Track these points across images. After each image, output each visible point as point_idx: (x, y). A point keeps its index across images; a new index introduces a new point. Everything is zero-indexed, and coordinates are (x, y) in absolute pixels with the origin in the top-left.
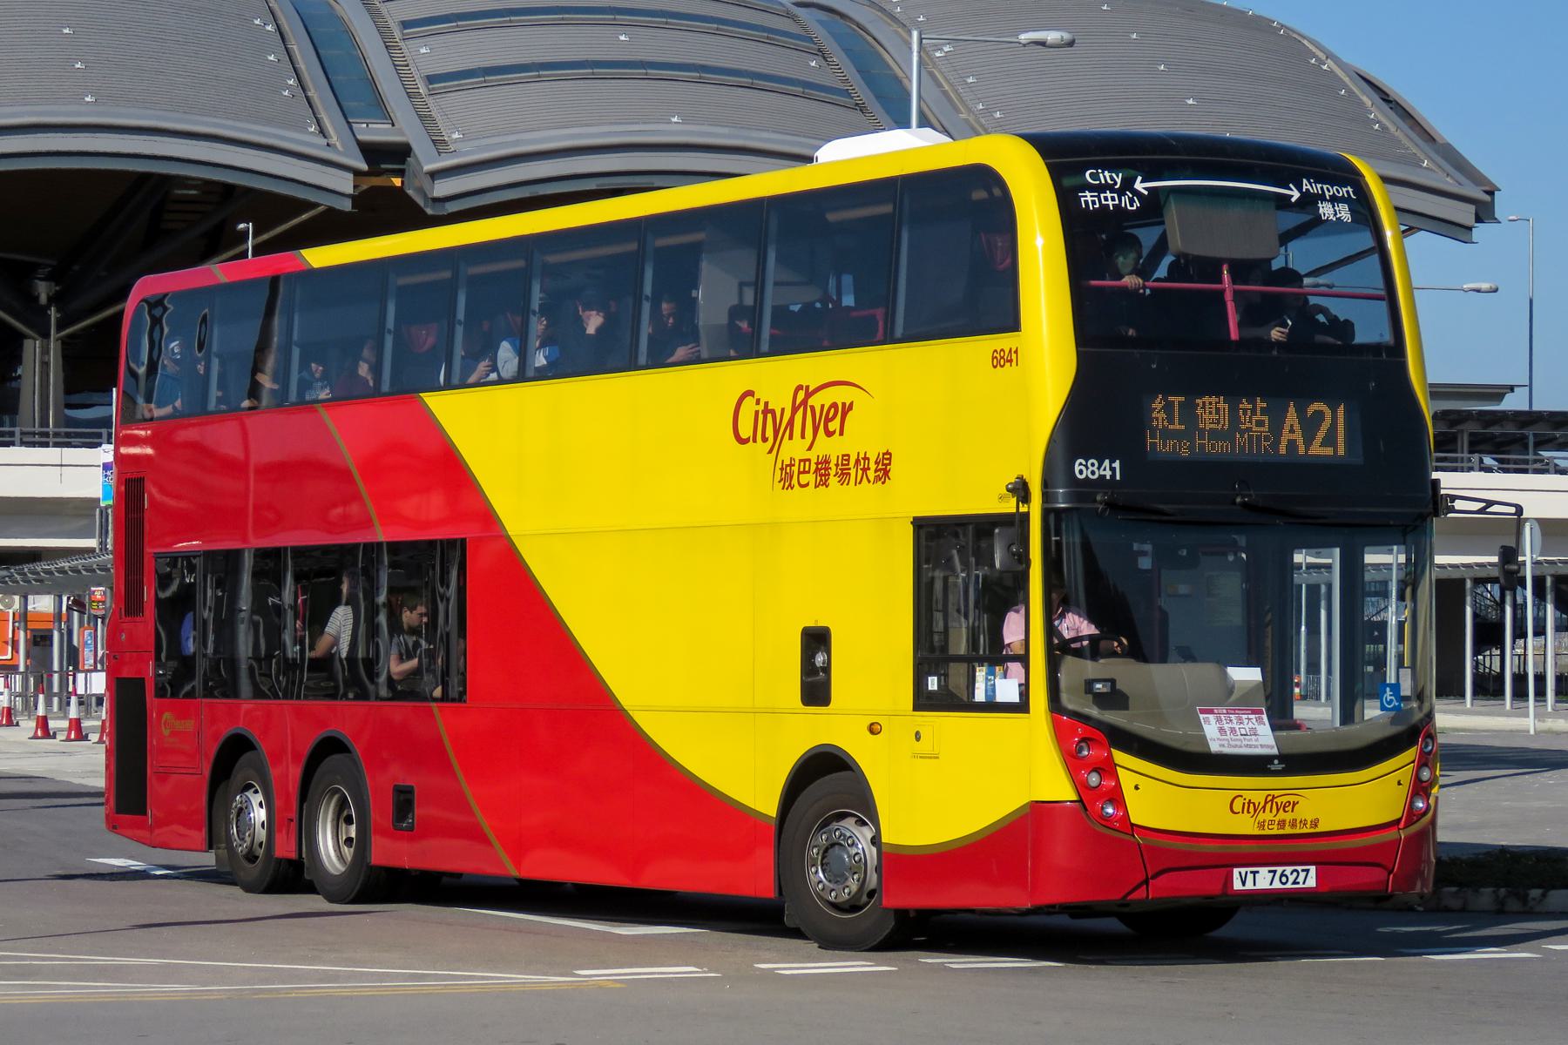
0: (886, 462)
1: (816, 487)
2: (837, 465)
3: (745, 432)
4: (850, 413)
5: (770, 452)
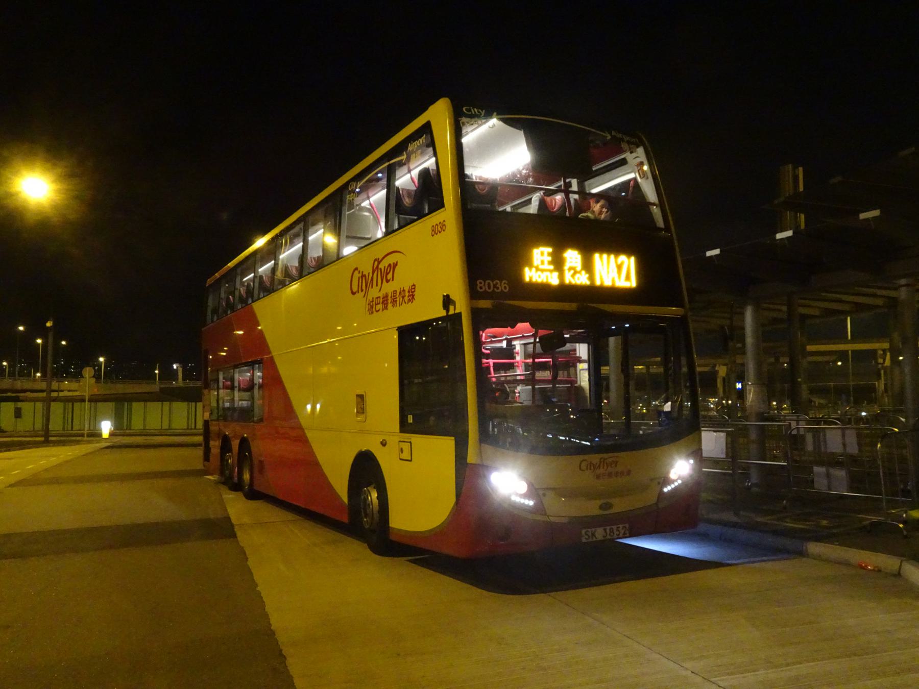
0: (413, 290)
1: (383, 310)
2: (391, 297)
3: (355, 289)
4: (397, 268)
5: (364, 296)
